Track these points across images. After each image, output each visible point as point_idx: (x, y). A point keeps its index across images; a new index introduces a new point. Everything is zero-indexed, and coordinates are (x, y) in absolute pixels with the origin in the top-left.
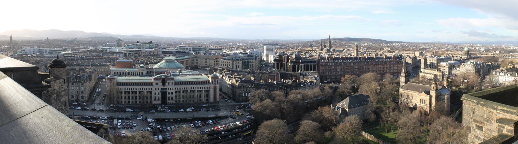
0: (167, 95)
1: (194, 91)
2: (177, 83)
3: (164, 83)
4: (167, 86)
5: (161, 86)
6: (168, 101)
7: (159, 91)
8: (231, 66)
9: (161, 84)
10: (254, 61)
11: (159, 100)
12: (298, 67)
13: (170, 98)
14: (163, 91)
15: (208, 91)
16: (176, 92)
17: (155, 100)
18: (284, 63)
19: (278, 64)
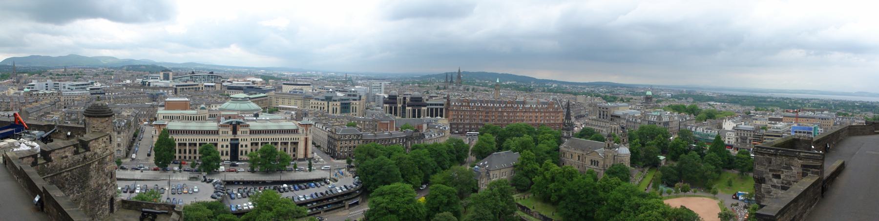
0: (240, 149)
1: (276, 144)
2: (252, 132)
3: (235, 132)
4: (240, 135)
5: (230, 135)
6: (240, 156)
7: (228, 143)
8: (326, 109)
9: (230, 133)
10: (357, 102)
11: (227, 154)
12: (419, 111)
15: (296, 144)
16: (252, 144)
17: (222, 154)
18: (399, 105)
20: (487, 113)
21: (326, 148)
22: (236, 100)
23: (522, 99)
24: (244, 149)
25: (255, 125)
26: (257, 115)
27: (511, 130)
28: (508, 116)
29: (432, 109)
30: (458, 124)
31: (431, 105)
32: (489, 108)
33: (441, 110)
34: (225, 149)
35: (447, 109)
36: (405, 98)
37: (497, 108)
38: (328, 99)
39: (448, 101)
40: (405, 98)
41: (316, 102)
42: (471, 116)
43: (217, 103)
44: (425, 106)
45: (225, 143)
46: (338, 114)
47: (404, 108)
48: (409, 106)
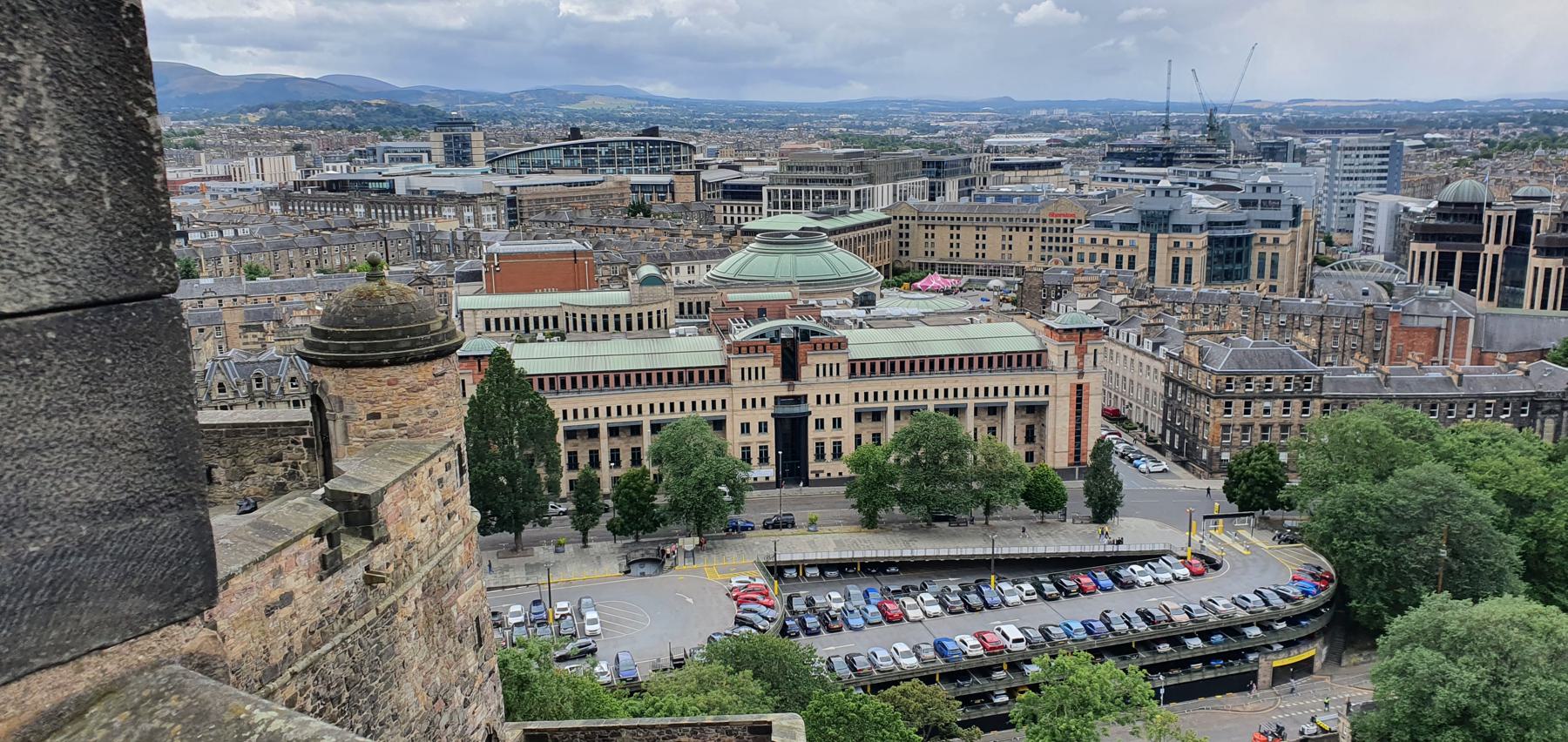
0: (813, 435)
1: (955, 411)
2: (859, 369)
3: (790, 372)
4: (809, 383)
5: (773, 385)
6: (813, 465)
7: (765, 415)
8: (1142, 263)
9: (774, 373)
10: (1285, 234)
11: (764, 459)
13: (828, 450)
14: (787, 410)
16: (858, 416)
18: (1491, 249)
19: (1446, 263)
21: (1156, 427)
22: (776, 239)
24: (828, 435)
25: (866, 343)
26: (866, 301)
34: (755, 439)
36: (1524, 216)
38: (1155, 222)
40: (1524, 216)
41: (1100, 234)
43: (690, 255)
45: (755, 417)
46: (1198, 285)
47: (1515, 261)
48: (1546, 251)
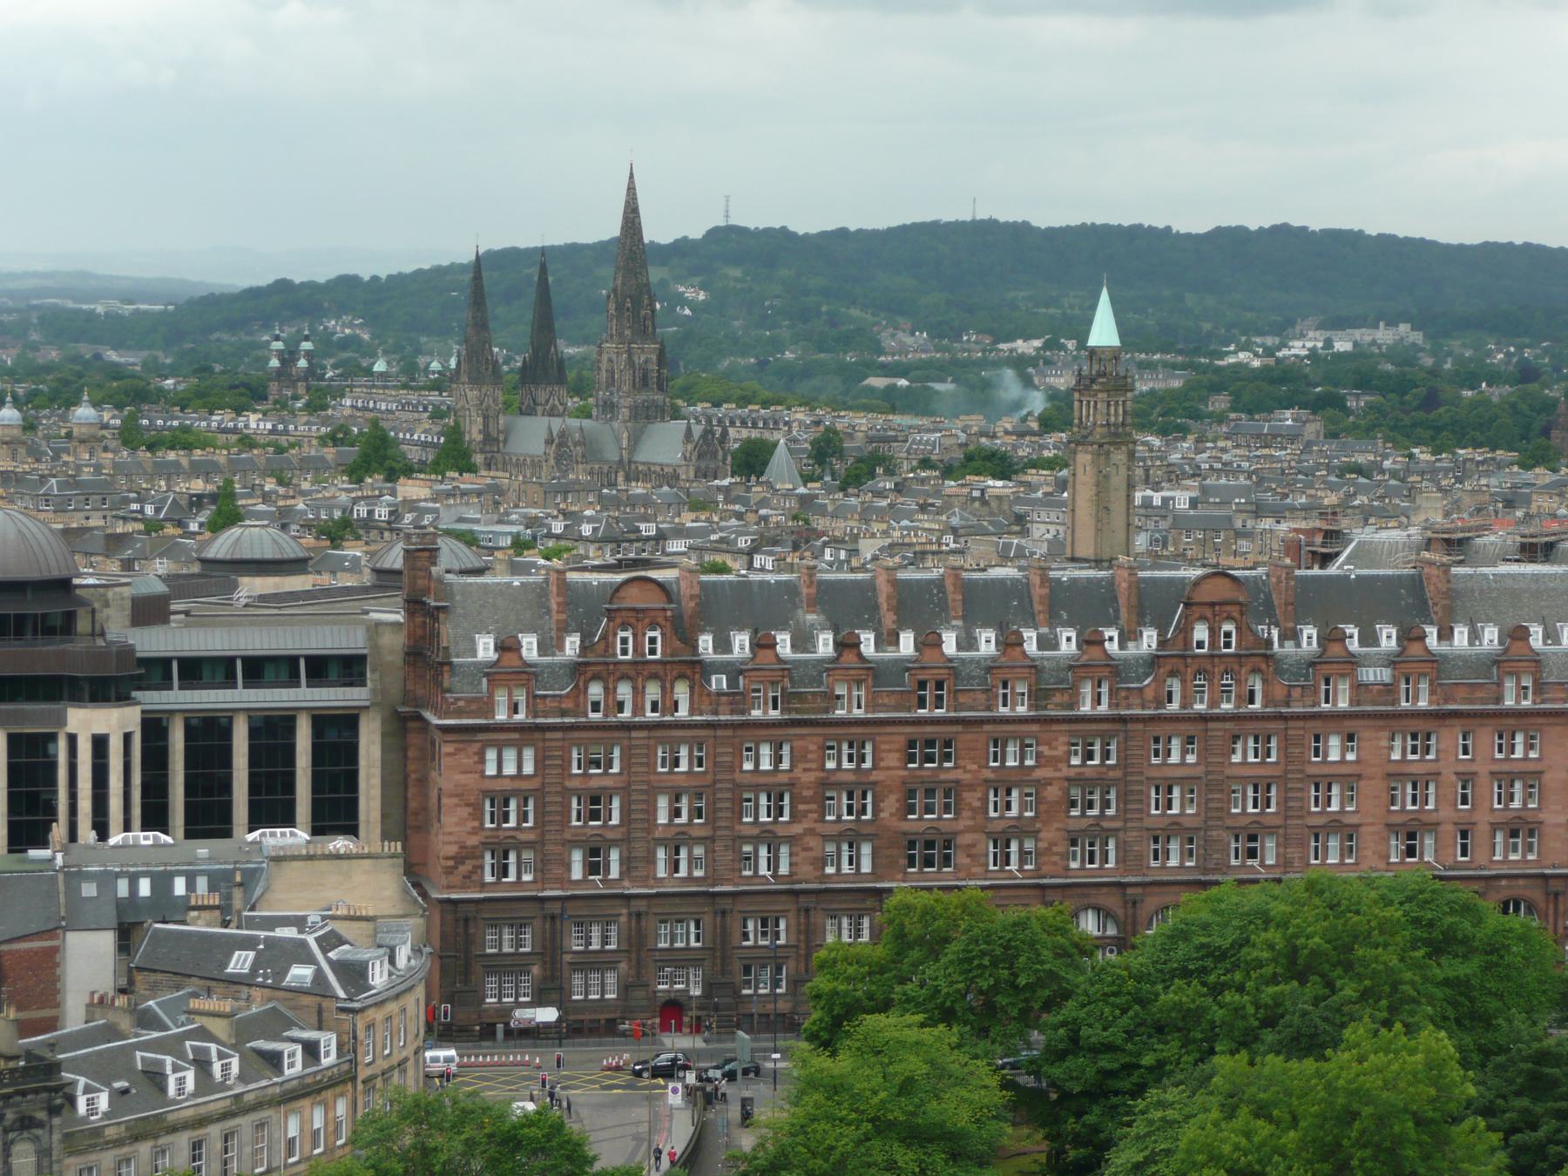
20: (924, 745)
23: (1382, 545)
27: (1214, 961)
28: (1212, 785)
29: (209, 735)
30: (553, 915)
31: (194, 671)
32: (927, 679)
33: (337, 735)
35: (404, 726)
37: (1048, 685)
39: (425, 611)
42: (719, 798)
44: (105, 690)
